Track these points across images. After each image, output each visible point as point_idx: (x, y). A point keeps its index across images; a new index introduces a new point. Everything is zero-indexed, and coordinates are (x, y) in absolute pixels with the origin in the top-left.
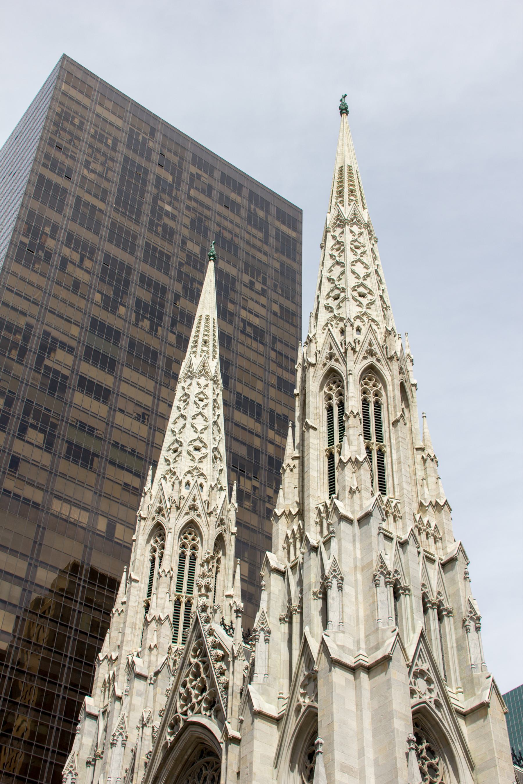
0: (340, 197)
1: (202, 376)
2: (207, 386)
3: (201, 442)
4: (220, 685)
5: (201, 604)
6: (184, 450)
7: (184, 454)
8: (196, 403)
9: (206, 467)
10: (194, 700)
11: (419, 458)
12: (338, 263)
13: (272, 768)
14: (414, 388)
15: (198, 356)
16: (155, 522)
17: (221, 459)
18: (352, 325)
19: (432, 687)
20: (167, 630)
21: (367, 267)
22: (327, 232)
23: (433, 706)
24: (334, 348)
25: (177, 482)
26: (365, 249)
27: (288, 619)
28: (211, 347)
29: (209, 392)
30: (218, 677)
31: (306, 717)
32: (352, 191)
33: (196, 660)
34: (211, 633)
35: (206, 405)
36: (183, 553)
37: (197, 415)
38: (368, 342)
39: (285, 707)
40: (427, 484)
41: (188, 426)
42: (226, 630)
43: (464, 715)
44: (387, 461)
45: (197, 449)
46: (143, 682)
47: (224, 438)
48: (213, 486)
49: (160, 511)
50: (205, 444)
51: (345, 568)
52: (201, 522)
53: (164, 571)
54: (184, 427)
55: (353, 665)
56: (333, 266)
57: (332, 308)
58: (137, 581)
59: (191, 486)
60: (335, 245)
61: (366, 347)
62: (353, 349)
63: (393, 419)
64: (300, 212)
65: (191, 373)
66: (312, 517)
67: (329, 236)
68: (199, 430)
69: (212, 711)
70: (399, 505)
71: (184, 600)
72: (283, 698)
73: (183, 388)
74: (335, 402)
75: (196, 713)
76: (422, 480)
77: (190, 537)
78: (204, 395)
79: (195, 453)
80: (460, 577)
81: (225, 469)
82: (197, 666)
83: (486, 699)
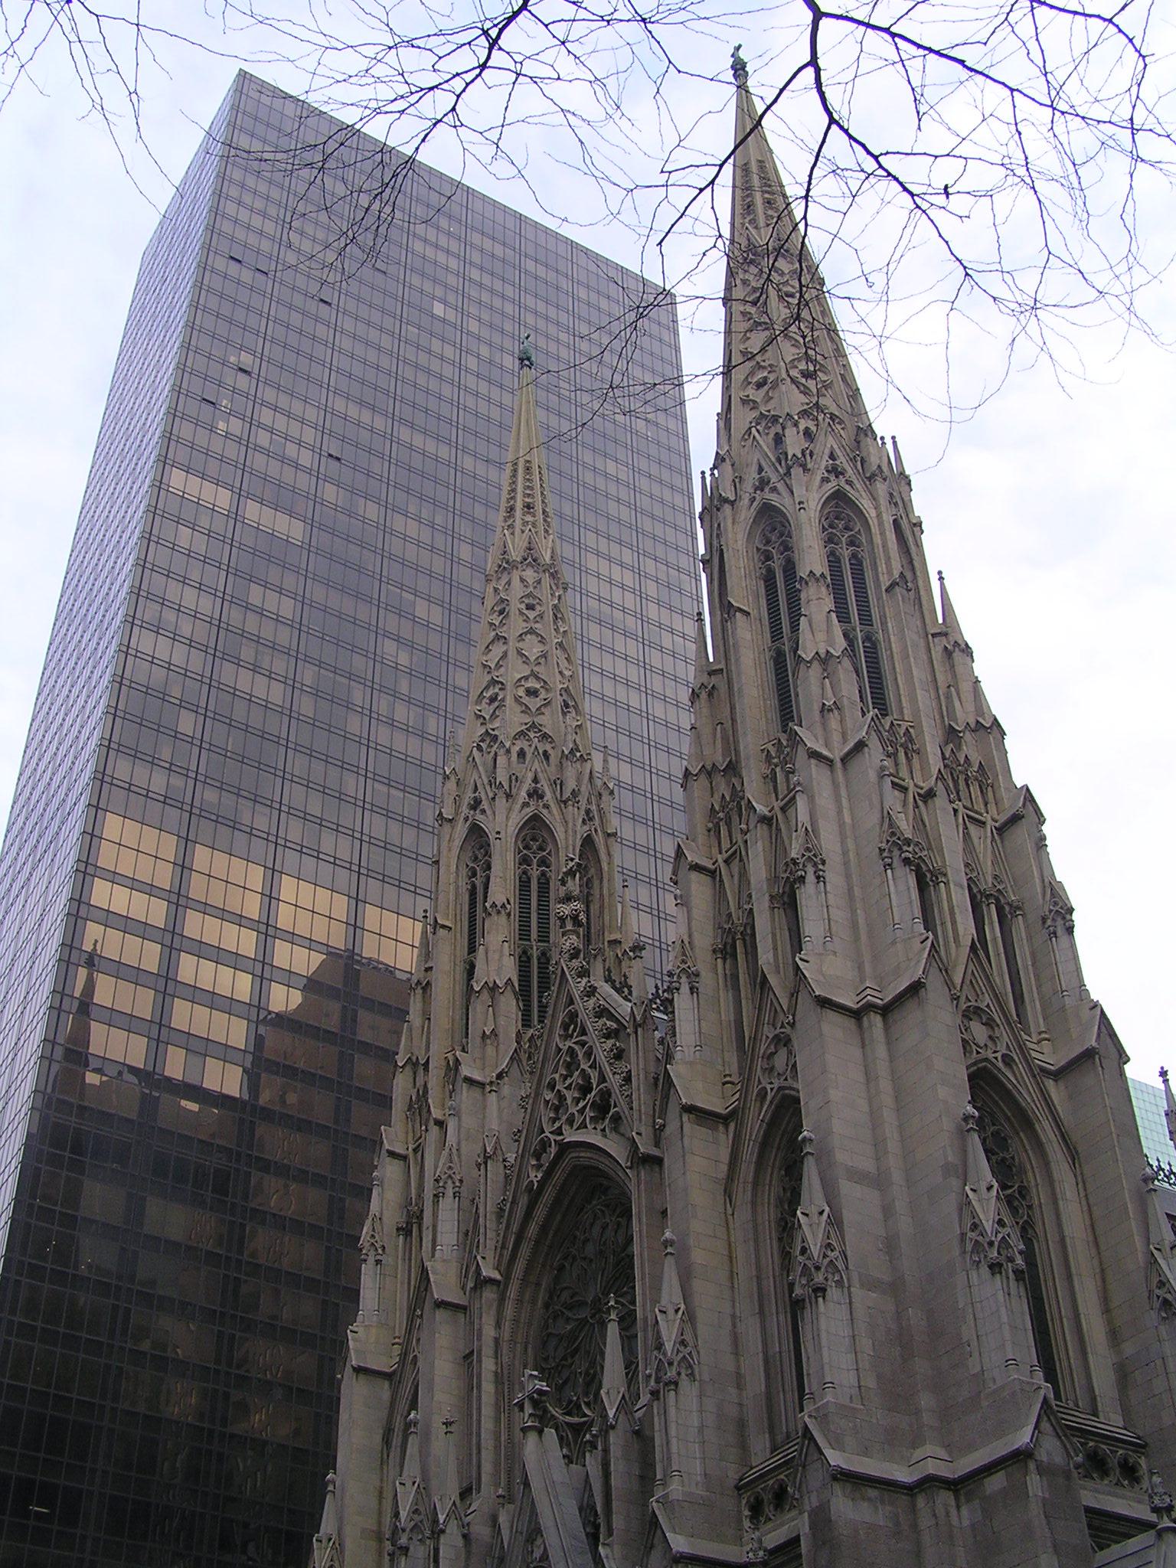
1: (527, 565)
2: (539, 582)
3: (538, 678)
4: (617, 1076)
7: (509, 701)
8: (521, 613)
11: (937, 653)
14: (916, 529)
15: (517, 531)
16: (468, 823)
18: (796, 425)
20: (509, 1005)
23: (1000, 1065)
25: (502, 751)
31: (777, 1107)
33: (569, 1043)
34: (591, 992)
35: (541, 616)
36: (525, 872)
37: (526, 633)
38: (827, 452)
39: (737, 1096)
40: (958, 694)
41: (512, 654)
42: (619, 991)
43: (1057, 1075)
44: (884, 655)
45: (532, 693)
48: (566, 752)
49: (476, 804)
50: (545, 682)
51: (829, 842)
52: (553, 817)
53: (494, 905)
54: (505, 655)
55: (855, 1007)
57: (754, 402)
59: (529, 756)
61: (825, 462)
63: (885, 582)
65: (507, 563)
68: (532, 659)
69: (607, 1121)
70: (911, 730)
71: (535, 953)
72: (732, 1083)
73: (496, 590)
74: (777, 565)
75: (577, 1129)
76: (949, 687)
77: (535, 846)
78: (535, 597)
79: (526, 700)
82: (571, 1052)
83: (1094, 1044)
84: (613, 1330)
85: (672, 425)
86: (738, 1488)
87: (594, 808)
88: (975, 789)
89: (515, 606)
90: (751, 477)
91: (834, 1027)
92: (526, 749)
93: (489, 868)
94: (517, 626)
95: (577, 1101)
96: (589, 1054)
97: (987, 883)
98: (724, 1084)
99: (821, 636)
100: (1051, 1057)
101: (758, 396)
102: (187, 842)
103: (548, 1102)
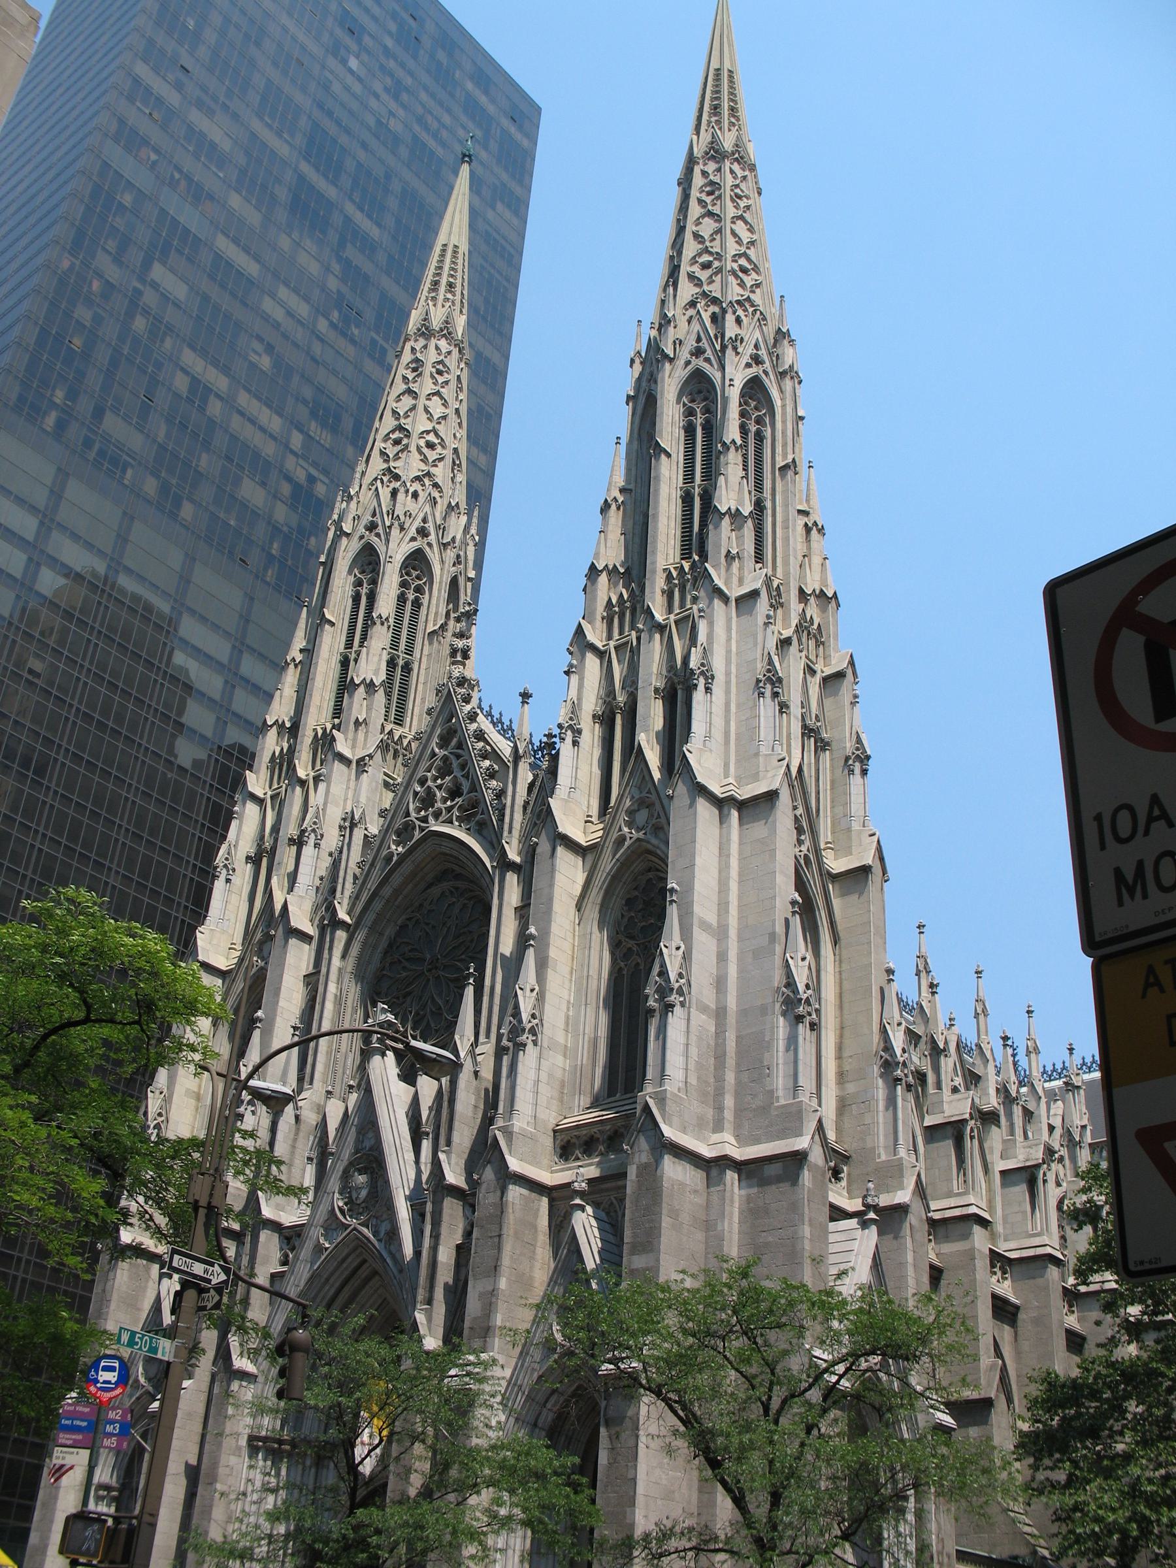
0: (715, 115)
2: (449, 353)
3: (437, 435)
5: (456, 674)
6: (415, 442)
7: (413, 448)
8: (432, 377)
9: (441, 473)
10: (439, 805)
12: (710, 214)
13: (573, 909)
17: (460, 465)
19: (803, 837)
21: (751, 230)
22: (691, 161)
24: (704, 340)
25: (402, 490)
26: (750, 202)
27: (606, 720)
28: (458, 297)
29: (452, 362)
30: (484, 780)
32: (733, 110)
37: (434, 394)
38: (753, 342)
41: (420, 408)
45: (431, 446)
46: (343, 767)
47: (465, 437)
49: (371, 527)
51: (718, 665)
52: (434, 556)
53: (380, 617)
54: (413, 408)
56: (703, 216)
57: (699, 279)
58: (332, 624)
60: (705, 185)
61: (750, 350)
62: (735, 349)
63: (780, 463)
64: (538, 110)
66: (657, 583)
67: (697, 170)
68: (436, 417)
69: (473, 824)
71: (401, 662)
77: (415, 573)
78: (445, 366)
79: (425, 450)
80: (847, 699)
81: (464, 483)
82: (445, 759)
84: (469, 992)
85: (515, 221)
86: (555, 1131)
87: (462, 553)
88: (812, 643)
89: (428, 369)
90: (691, 343)
91: (704, 809)
92: (420, 493)
93: (374, 582)
94: (428, 386)
95: (445, 800)
96: (463, 767)
97: (811, 722)
98: (586, 822)
99: (733, 495)
100: (836, 864)
101: (704, 275)
102: (63, 474)
103: (416, 794)
